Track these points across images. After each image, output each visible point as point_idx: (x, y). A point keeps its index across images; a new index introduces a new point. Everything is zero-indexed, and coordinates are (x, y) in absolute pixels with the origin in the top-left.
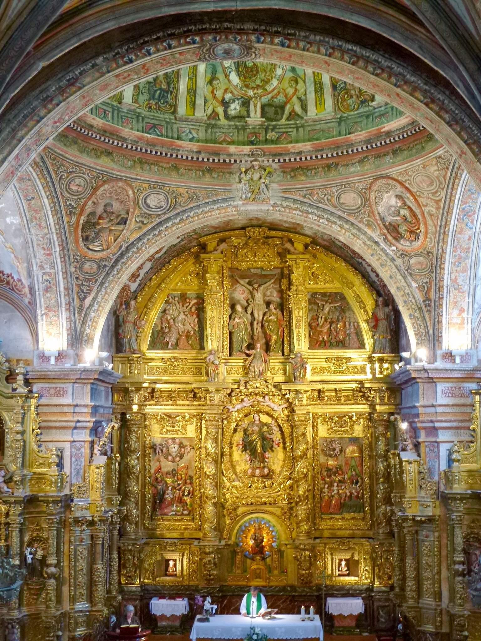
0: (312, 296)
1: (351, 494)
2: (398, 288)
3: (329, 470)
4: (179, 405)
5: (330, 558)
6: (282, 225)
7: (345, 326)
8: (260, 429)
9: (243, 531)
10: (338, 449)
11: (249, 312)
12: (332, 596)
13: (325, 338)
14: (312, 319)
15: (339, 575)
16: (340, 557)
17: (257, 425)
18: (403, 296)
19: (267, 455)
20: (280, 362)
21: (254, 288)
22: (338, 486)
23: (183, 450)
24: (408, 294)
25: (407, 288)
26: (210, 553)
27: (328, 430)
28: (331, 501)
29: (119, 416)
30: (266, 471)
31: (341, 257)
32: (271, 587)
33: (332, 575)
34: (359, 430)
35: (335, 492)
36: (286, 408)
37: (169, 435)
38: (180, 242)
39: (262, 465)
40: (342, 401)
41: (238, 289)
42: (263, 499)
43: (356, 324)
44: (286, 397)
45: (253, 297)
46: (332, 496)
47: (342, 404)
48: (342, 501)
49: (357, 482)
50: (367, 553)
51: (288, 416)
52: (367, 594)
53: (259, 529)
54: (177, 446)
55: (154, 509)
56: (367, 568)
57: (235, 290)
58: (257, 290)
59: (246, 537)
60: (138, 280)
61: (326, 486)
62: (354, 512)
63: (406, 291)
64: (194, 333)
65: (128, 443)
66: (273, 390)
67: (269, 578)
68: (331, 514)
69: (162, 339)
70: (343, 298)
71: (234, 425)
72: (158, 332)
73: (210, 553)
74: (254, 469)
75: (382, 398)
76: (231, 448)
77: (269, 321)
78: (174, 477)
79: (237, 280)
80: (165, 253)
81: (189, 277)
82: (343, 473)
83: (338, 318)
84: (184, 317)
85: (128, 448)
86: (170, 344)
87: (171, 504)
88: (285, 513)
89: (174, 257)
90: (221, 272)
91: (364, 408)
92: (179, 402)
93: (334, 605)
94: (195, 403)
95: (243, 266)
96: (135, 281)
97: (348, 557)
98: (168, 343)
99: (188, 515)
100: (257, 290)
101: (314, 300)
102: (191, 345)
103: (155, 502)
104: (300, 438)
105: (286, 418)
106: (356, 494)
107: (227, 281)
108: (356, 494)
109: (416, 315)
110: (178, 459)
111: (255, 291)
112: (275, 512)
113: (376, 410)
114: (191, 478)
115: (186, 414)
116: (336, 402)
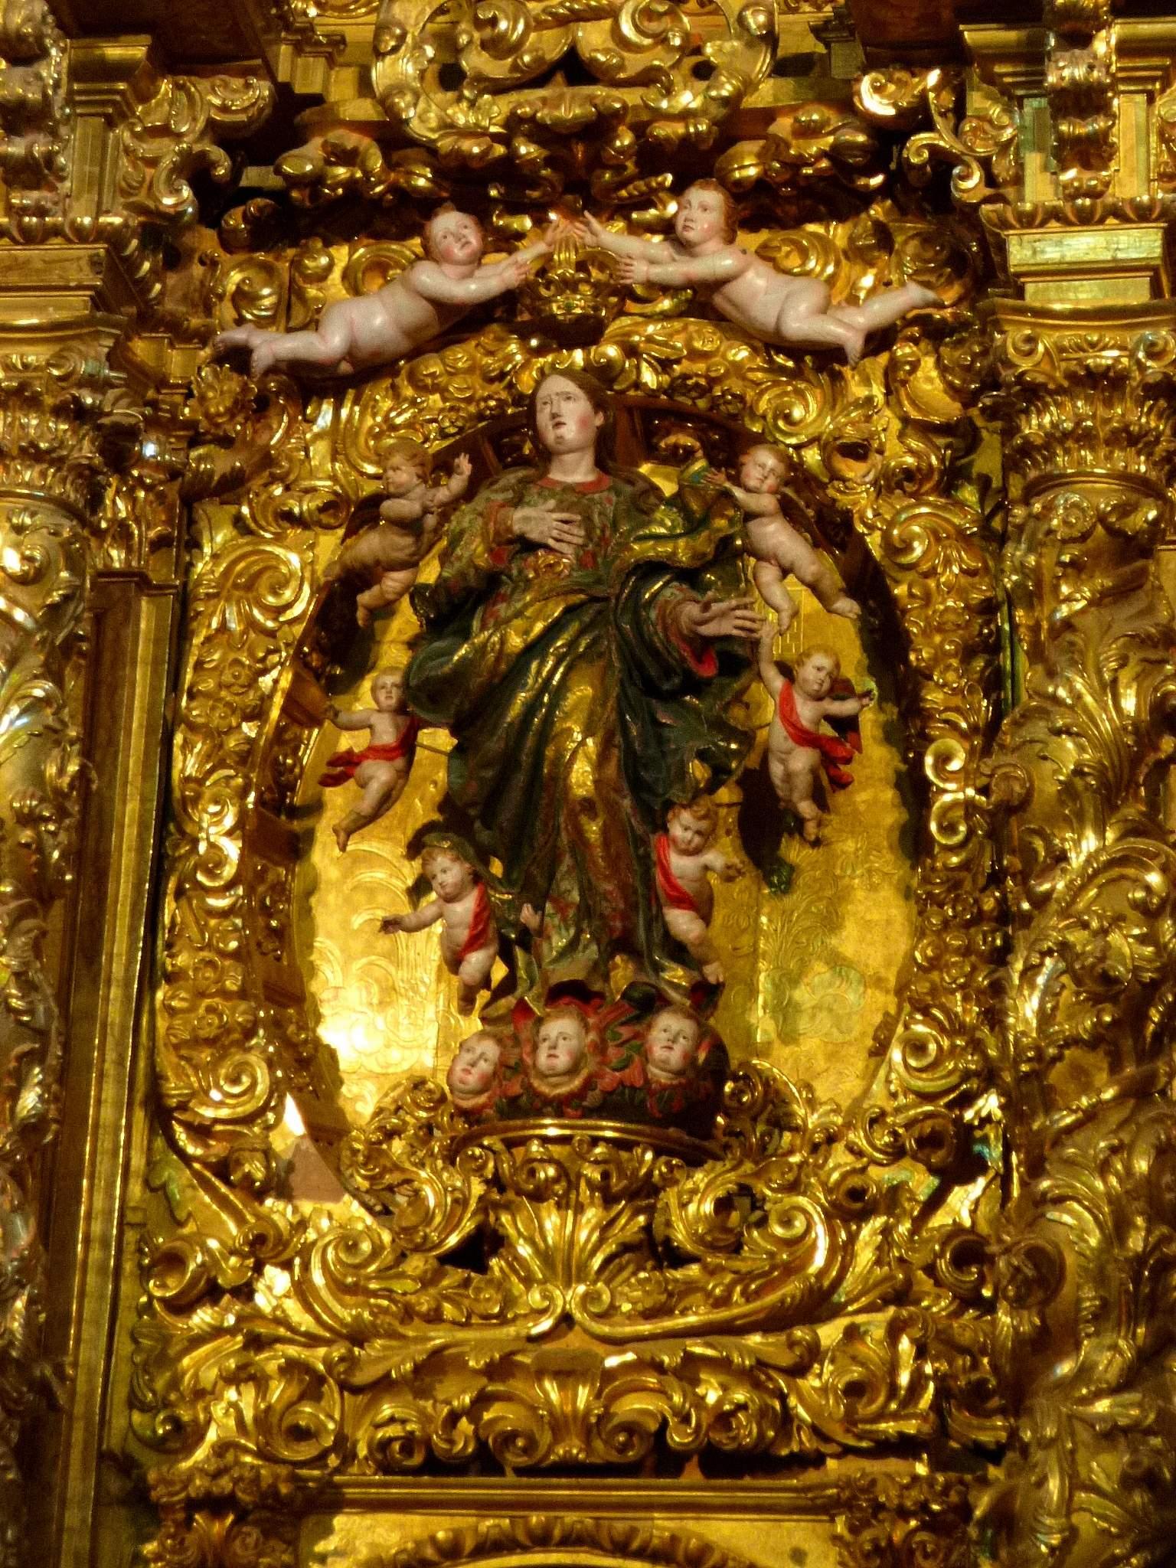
17: (573, 498)
19: (695, 850)
30: (669, 1039)
36: (933, 332)
39: (622, 973)
42: (632, 1405)
44: (917, 148)
51: (962, 436)
74: (507, 1011)
76: (279, 834)
104: (1073, 600)
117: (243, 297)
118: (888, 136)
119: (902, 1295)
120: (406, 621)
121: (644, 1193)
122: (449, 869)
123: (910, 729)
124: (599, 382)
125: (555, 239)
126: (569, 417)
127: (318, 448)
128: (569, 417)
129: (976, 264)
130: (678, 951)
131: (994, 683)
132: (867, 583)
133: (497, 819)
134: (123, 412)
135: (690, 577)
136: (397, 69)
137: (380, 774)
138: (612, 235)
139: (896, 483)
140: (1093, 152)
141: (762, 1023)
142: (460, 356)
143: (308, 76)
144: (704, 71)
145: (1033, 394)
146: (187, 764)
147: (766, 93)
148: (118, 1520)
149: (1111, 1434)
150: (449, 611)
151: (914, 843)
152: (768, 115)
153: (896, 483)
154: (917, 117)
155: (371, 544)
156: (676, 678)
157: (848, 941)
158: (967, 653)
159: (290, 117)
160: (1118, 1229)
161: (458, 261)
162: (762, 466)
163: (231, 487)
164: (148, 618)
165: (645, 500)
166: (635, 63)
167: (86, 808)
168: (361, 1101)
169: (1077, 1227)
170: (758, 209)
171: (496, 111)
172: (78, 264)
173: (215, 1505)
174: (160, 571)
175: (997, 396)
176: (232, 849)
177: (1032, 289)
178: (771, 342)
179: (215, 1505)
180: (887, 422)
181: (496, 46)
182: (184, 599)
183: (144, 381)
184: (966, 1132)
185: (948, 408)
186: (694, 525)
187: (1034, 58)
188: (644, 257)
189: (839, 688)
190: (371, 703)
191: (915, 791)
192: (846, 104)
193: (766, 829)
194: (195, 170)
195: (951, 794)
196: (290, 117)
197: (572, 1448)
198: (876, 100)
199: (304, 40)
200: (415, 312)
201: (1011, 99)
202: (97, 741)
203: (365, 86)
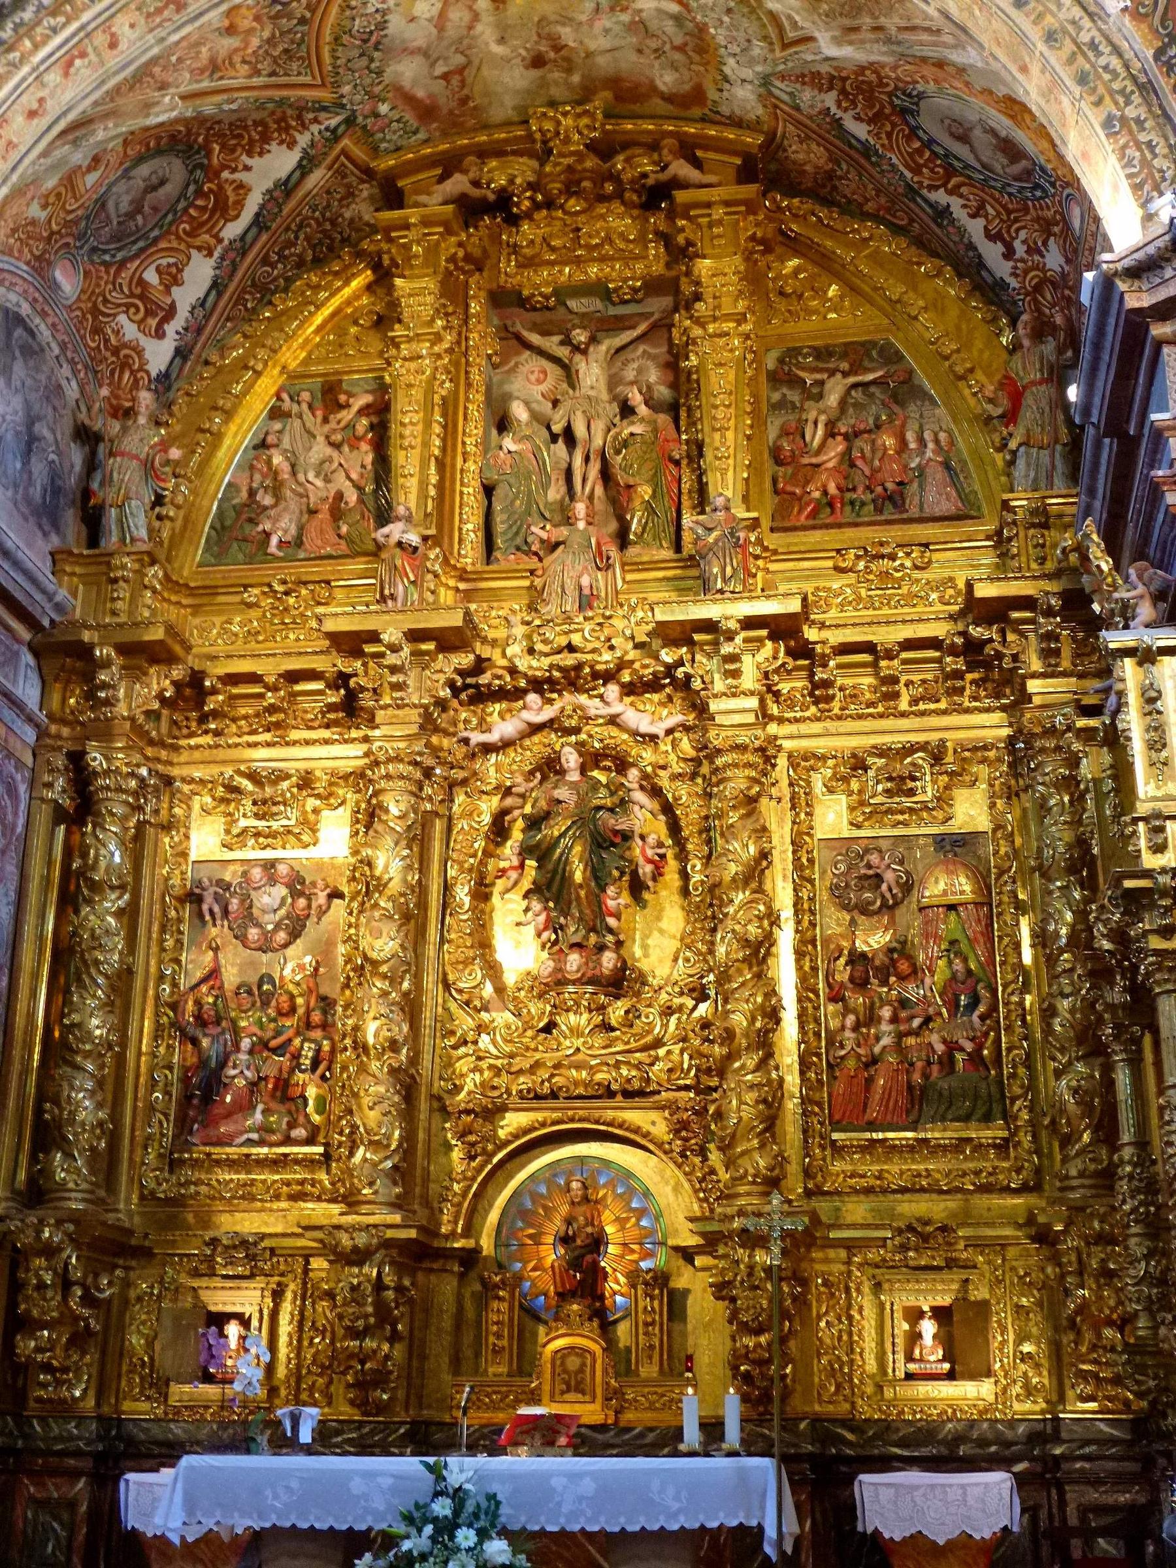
0: (781, 361)
1: (952, 1047)
2: (1050, 37)
3: (857, 959)
4: (295, 743)
5: (870, 1312)
6: (654, 89)
7: (903, 444)
8: (581, 801)
9: (526, 1215)
10: (889, 876)
11: (557, 428)
12: (884, 1464)
13: (832, 489)
14: (785, 432)
15: (909, 1376)
16: (911, 1301)
17: (574, 786)
18: (1071, 60)
19: (616, 898)
20: (668, 579)
21: (576, 349)
22: (894, 1020)
23: (302, 902)
24: (1093, 46)
25: (1086, 23)
26: (358, 1257)
27: (852, 809)
28: (870, 1081)
29: (60, 762)
30: (608, 960)
31: (877, 218)
32: (628, 1430)
33: (881, 1380)
34: (971, 811)
35: (886, 1041)
36: (687, 729)
37: (251, 853)
38: (304, 168)
39: (593, 939)
40: (904, 705)
41: (523, 369)
42: (599, 1077)
43: (942, 436)
44: (680, 673)
45: (570, 375)
46: (874, 1061)
47: (903, 715)
48: (917, 1078)
49: (975, 1001)
50: (1026, 1286)
51: (697, 762)
52: (1034, 1456)
53: (586, 1199)
54: (281, 891)
55: (183, 1125)
56: (1027, 1348)
57: (513, 370)
58: (584, 352)
59: (537, 1239)
60: (171, 329)
61: (850, 1019)
62: (966, 1118)
63: (1085, 37)
64: (361, 501)
65: (84, 855)
66: (632, 655)
67: (618, 1393)
68: (872, 1126)
69: (248, 528)
70: (890, 356)
71: (488, 807)
72: (238, 510)
73: (358, 1257)
75: (1049, 654)
76: (482, 894)
77: (625, 443)
78: (265, 1004)
79: (518, 338)
80: (259, 222)
81: (353, 330)
82: (915, 972)
83: (877, 418)
84: (329, 451)
85: (82, 873)
86: (274, 540)
87: (244, 1106)
88: (684, 1125)
89: (300, 264)
90: (453, 294)
91: (991, 725)
92: (295, 735)
93: (886, 1495)
94: (354, 734)
95: (540, 282)
96: (160, 334)
97: (945, 1300)
98: (267, 535)
99: (310, 1141)
100: (584, 352)
101: (785, 377)
102: (349, 539)
103: (186, 1099)
104: (734, 817)
105: (688, 768)
106: (969, 1046)
107: (482, 339)
108: (969, 1046)
109: (1131, 112)
110: (282, 936)
111: (578, 357)
112: (646, 1127)
113: (1029, 698)
114: (327, 1003)
115: (318, 773)
116: (880, 709)
117: (466, 721)
118: (670, 669)
119: (684, 1040)
120: (520, 824)
121: (602, 1008)
122: (537, 906)
123: (683, 856)
124: (580, 745)
125: (567, 700)
126: (571, 759)
127: (491, 769)
128: (571, 759)
129: (701, 709)
130: (610, 931)
131: (709, 842)
132: (668, 809)
133: (551, 888)
134: (429, 762)
135: (611, 810)
136: (514, 650)
137: (514, 875)
138: (583, 699)
139: (675, 777)
140: (736, 674)
141: (638, 952)
142: (536, 739)
143: (485, 652)
144: (612, 648)
145: (719, 752)
146: (451, 873)
147: (632, 655)
148: (437, 1117)
149: (752, 1087)
150: (534, 823)
151: (685, 892)
152: (632, 662)
153: (675, 777)
154: (680, 663)
155: (509, 801)
156: (607, 843)
157: (664, 924)
158: (700, 832)
159: (481, 664)
160: (753, 1020)
161: (535, 709)
162: (633, 773)
163: (464, 782)
164: (439, 825)
165: (596, 785)
166: (590, 646)
167: (421, 889)
168: (510, 978)
169: (739, 1020)
170: (629, 690)
171: (546, 662)
172: (414, 715)
173: (468, 1112)
174: (442, 810)
175: (706, 753)
176: (467, 900)
177: (719, 719)
178: (635, 733)
179: (468, 1112)
180: (672, 757)
181: (545, 642)
182: (450, 819)
183: (435, 751)
184: (703, 987)
185: (692, 753)
186: (612, 794)
187: (716, 643)
188: (593, 706)
189: (660, 845)
190: (510, 850)
191: (685, 876)
192: (657, 658)
193: (637, 888)
194: (451, 684)
195: (696, 878)
196: (481, 664)
197: (581, 1091)
198: (668, 656)
199: (484, 640)
200: (522, 726)
201: (709, 657)
202: (424, 869)
203: (504, 655)
